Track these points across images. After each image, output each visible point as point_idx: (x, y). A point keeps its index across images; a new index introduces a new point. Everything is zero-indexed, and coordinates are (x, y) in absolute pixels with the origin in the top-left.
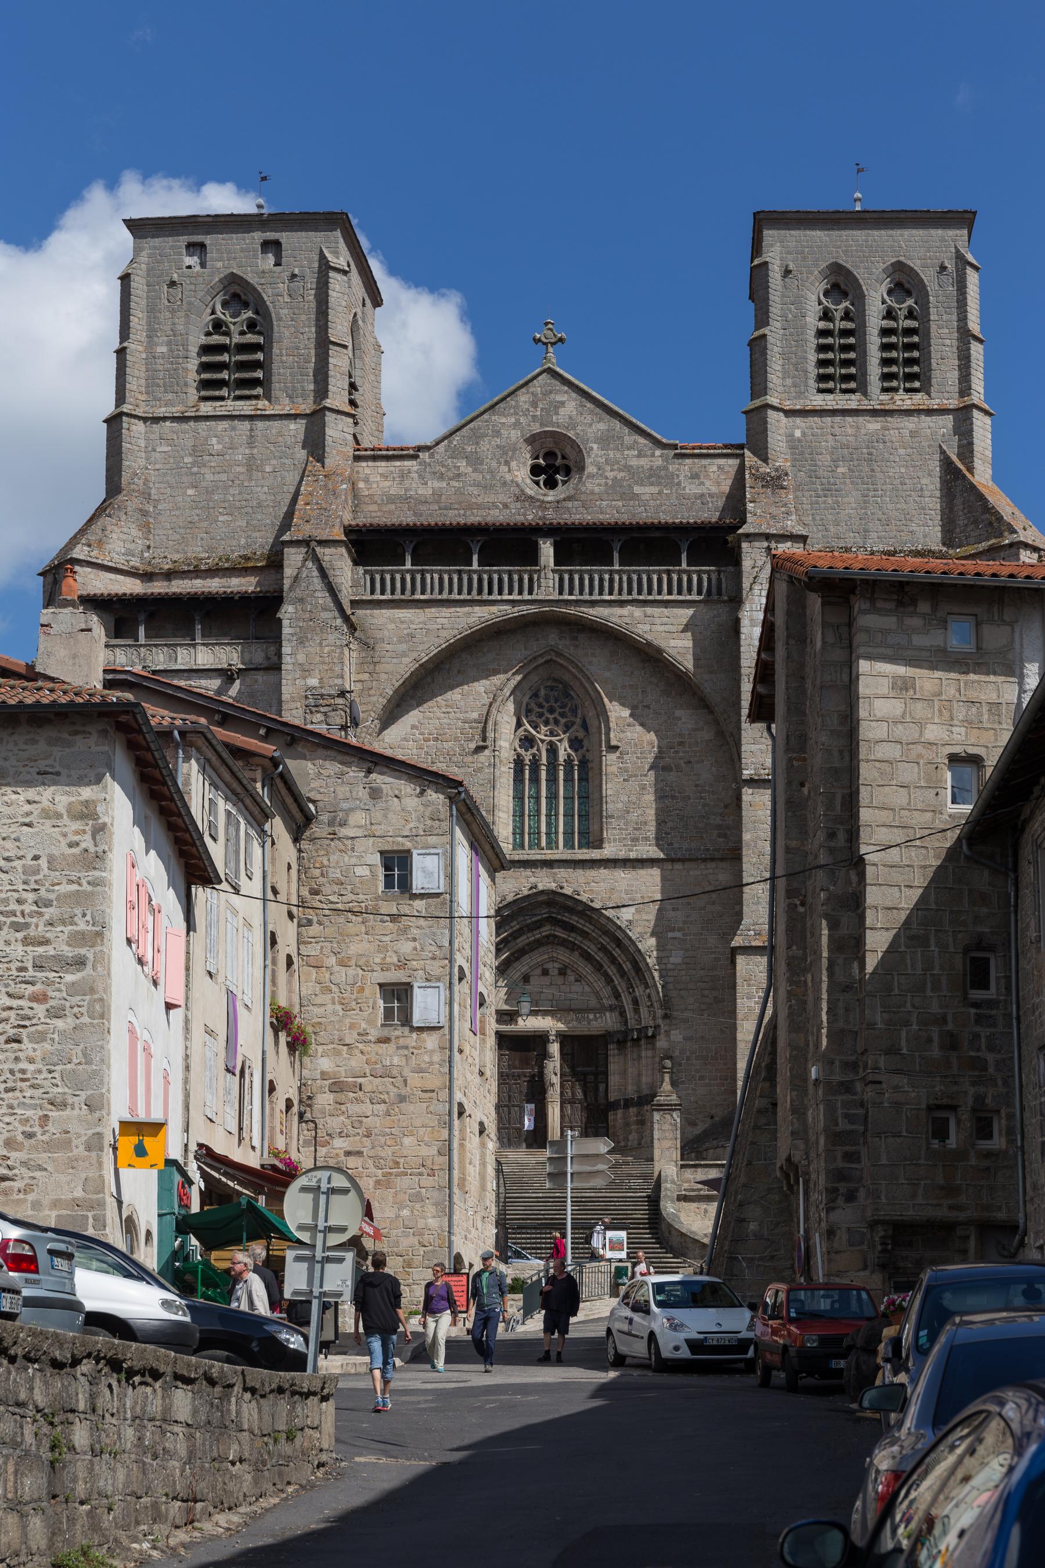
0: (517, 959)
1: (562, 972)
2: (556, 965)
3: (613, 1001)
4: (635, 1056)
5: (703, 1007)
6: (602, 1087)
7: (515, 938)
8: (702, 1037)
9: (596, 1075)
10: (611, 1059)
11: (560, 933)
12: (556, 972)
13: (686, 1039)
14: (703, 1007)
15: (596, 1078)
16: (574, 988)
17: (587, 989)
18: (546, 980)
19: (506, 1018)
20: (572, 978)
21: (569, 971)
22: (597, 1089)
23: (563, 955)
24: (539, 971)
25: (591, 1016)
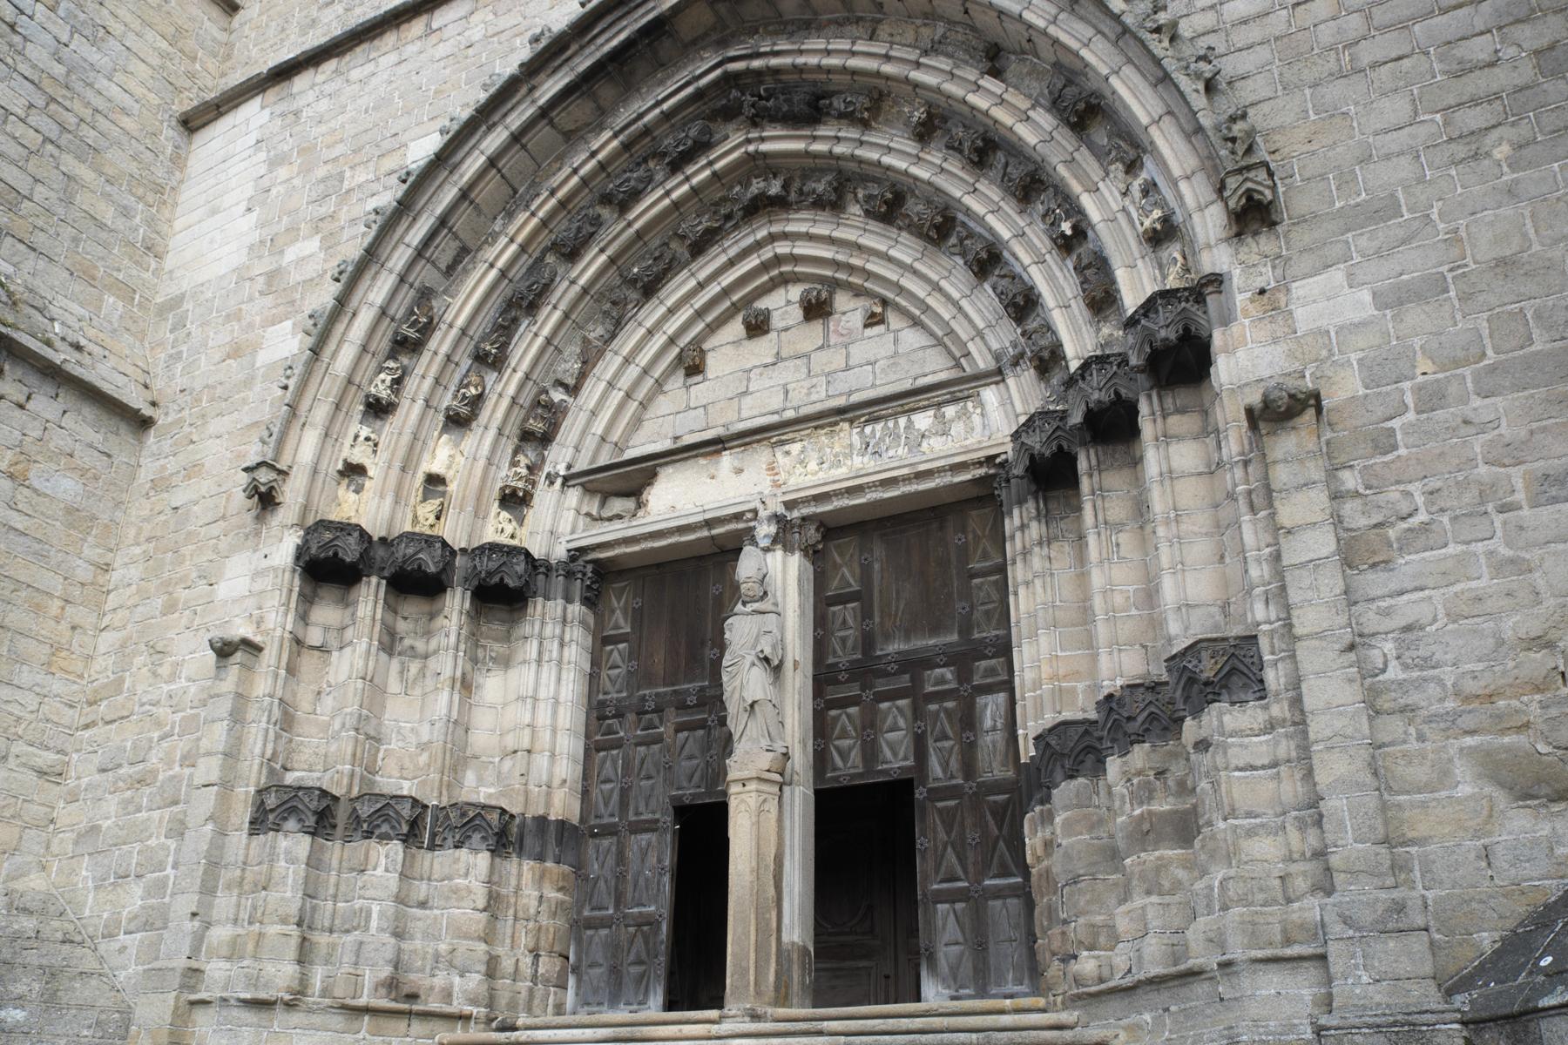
0: (649, 289)
1: (816, 310)
2: (795, 292)
3: (1004, 336)
4: (1117, 509)
5: (1473, 118)
6: (991, 708)
7: (624, 208)
8: (1501, 262)
9: (962, 659)
10: (1017, 573)
11: (780, 142)
12: (797, 313)
13: (1393, 299)
14: (1473, 118)
15: (964, 675)
16: (858, 352)
17: (912, 338)
18: (763, 348)
19: (618, 505)
20: (857, 319)
21: (842, 301)
22: (968, 720)
23: (809, 235)
24: (736, 328)
25: (923, 420)
